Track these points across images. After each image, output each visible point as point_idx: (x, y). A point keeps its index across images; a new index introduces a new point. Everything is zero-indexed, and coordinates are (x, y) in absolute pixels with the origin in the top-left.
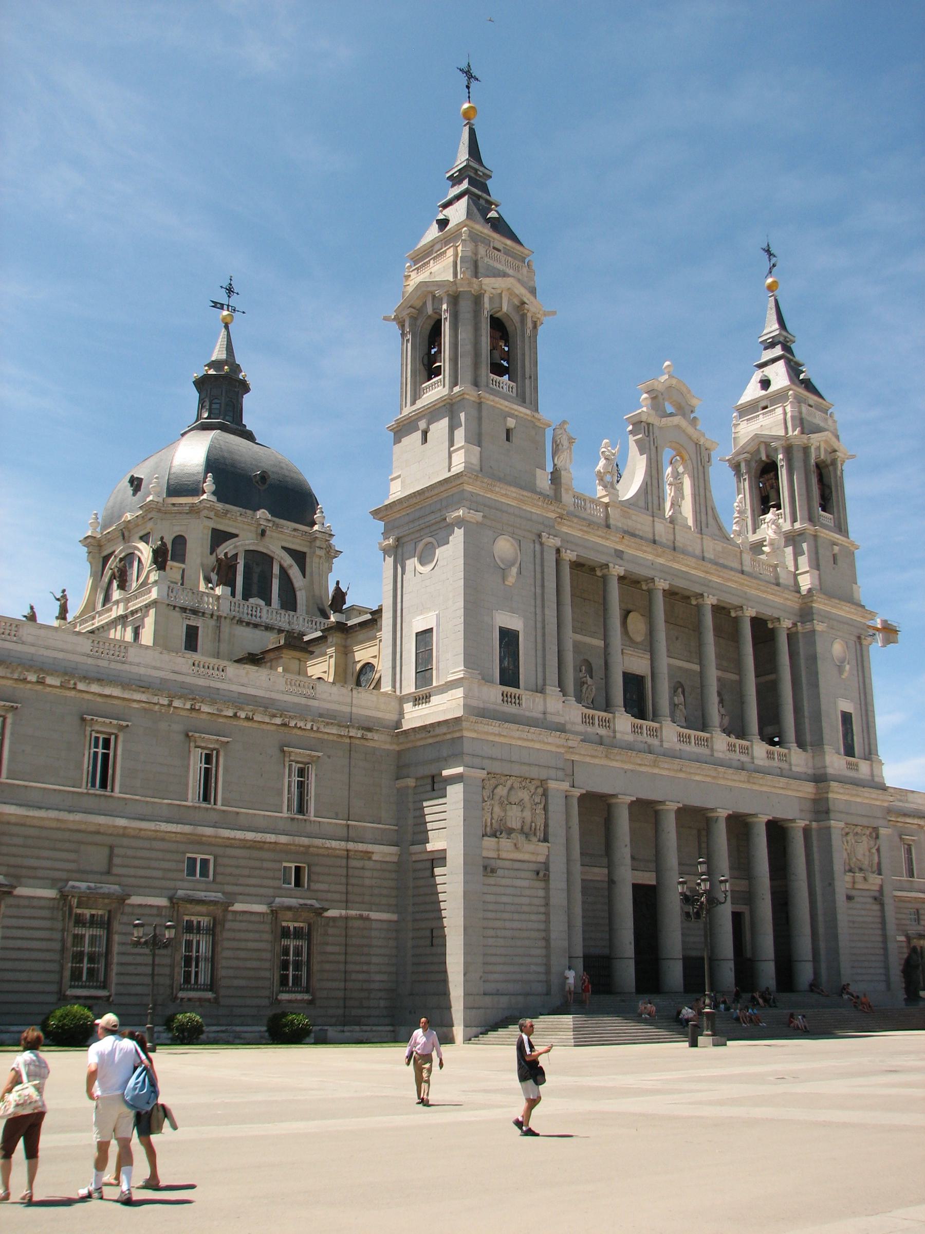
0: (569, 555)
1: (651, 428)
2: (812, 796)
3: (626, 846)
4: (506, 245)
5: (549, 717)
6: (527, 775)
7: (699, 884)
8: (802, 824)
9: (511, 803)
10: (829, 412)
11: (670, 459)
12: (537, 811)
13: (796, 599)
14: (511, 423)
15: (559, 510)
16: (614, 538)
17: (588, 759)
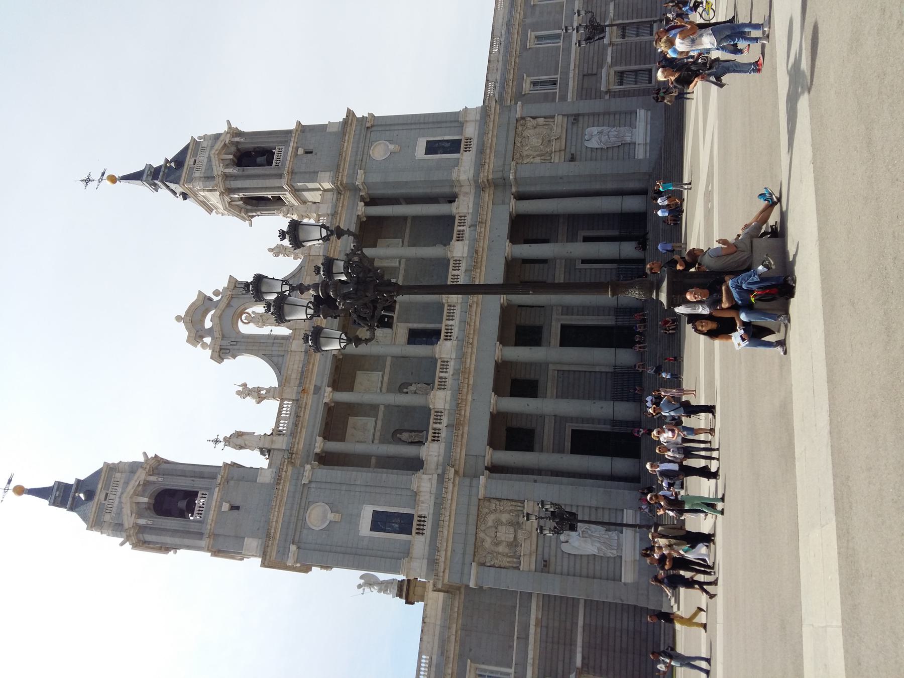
0: (319, 445)
1: (223, 347)
2: (492, 188)
3: (528, 405)
4: (102, 488)
5: (434, 490)
6: (475, 518)
7: (546, 510)
8: (513, 202)
9: (496, 536)
10: (198, 140)
11: (247, 325)
12: (502, 508)
13: (342, 196)
14: (226, 507)
15: (285, 467)
16: (304, 402)
17: (465, 441)
